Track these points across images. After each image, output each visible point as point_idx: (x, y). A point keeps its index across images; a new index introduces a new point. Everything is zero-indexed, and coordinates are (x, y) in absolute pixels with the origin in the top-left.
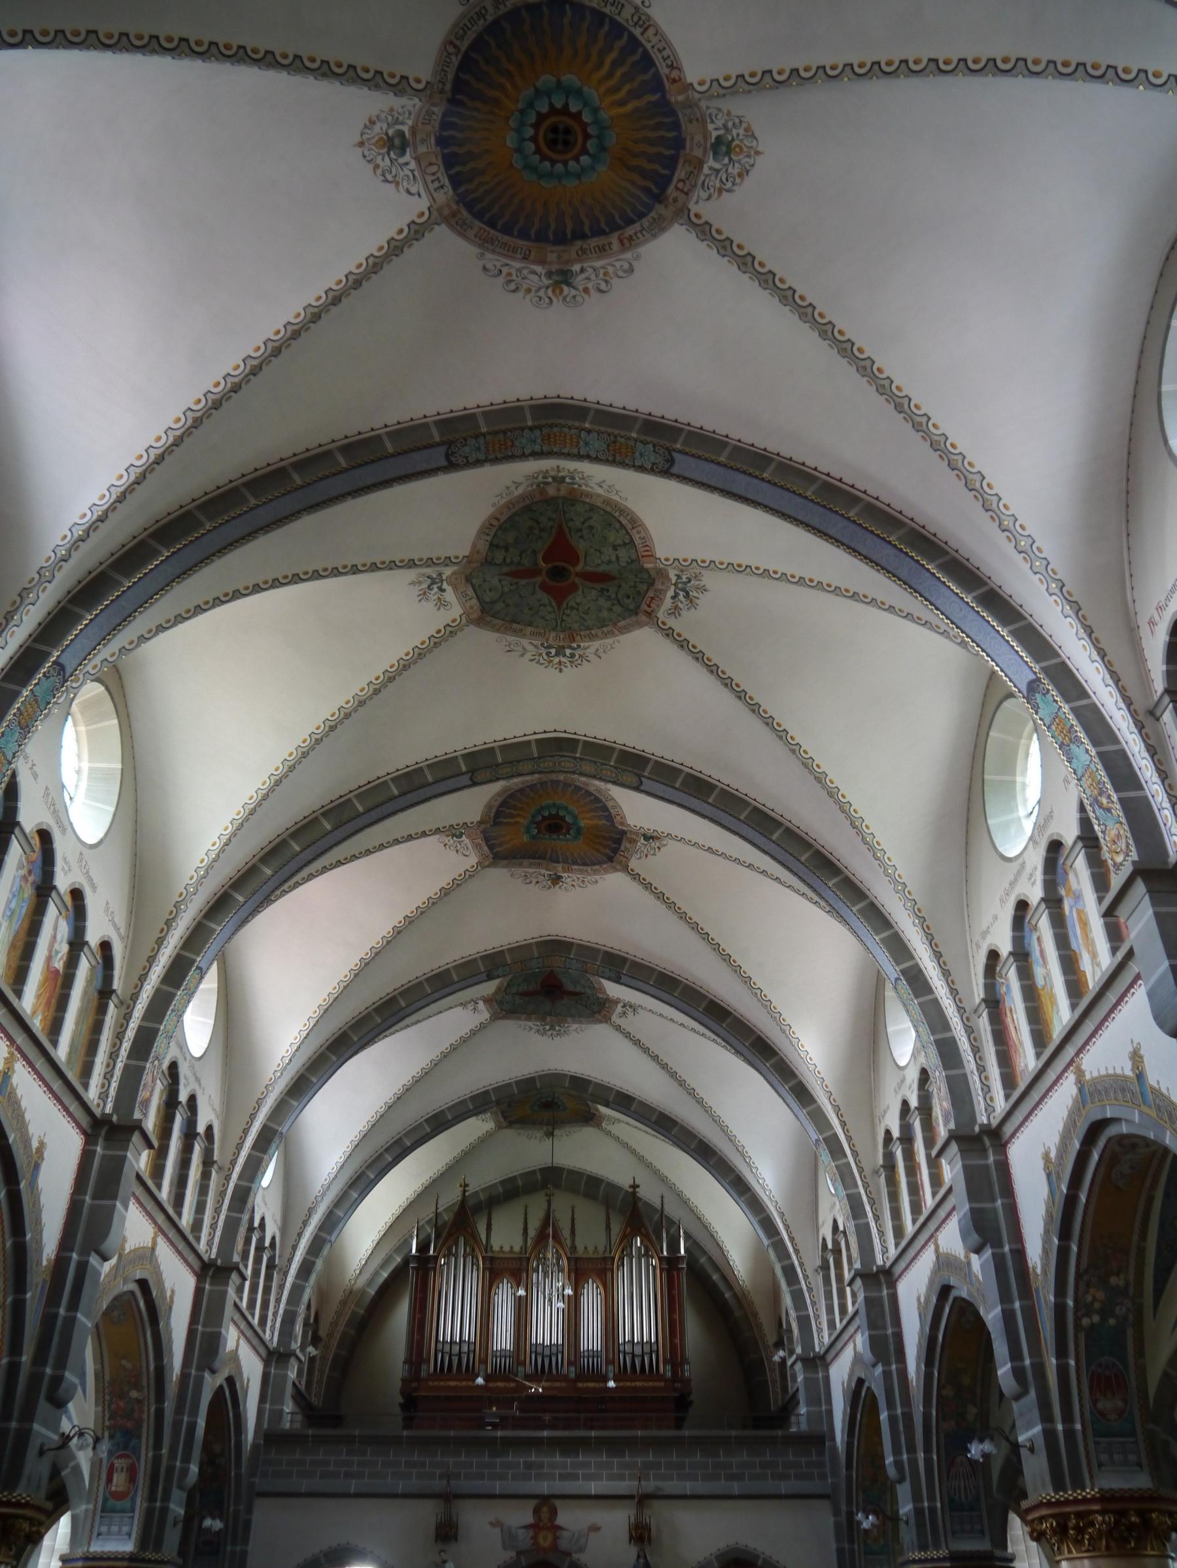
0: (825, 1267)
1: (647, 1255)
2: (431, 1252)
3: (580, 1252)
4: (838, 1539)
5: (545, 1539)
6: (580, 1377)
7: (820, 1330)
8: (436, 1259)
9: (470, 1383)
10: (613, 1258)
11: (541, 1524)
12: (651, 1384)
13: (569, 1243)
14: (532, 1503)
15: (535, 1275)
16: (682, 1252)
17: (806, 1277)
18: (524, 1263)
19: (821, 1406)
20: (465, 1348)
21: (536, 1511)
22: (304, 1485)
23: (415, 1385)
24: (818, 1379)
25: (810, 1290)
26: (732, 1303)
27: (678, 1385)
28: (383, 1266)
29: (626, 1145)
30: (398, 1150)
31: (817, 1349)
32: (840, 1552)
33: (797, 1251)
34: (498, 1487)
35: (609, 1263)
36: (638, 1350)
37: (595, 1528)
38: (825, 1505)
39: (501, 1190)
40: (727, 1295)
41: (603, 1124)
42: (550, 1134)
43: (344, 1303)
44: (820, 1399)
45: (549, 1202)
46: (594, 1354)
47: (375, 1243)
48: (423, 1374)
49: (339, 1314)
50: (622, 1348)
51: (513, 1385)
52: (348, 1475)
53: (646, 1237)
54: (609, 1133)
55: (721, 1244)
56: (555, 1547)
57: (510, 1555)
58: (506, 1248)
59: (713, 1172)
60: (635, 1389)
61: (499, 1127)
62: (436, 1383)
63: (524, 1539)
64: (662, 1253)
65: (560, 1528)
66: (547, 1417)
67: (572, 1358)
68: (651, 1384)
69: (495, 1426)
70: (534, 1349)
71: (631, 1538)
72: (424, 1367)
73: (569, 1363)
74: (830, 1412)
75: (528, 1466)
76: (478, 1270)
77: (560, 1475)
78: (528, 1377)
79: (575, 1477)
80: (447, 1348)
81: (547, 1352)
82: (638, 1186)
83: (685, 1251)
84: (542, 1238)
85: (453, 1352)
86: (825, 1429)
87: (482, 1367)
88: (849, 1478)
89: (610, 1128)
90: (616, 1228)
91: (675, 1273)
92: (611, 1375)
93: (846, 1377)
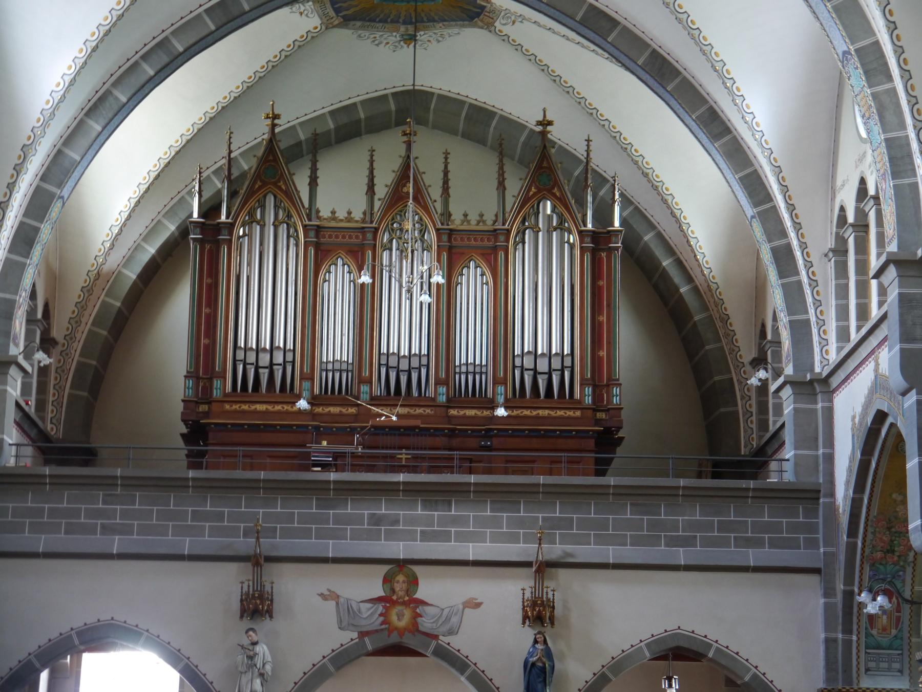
0: (840, 251)
1: (560, 227)
2: (223, 218)
3: (457, 221)
4: (828, 626)
5: (400, 616)
6: (452, 402)
7: (824, 343)
8: (231, 227)
9: (287, 407)
10: (509, 231)
11: (395, 598)
12: (560, 413)
13: (439, 206)
14: (385, 568)
15: (386, 254)
16: (617, 223)
17: (809, 265)
18: (369, 236)
19: (817, 449)
20: (279, 358)
21: (388, 580)
22: (42, 543)
23: (203, 408)
24: (816, 410)
25: (814, 283)
26: (691, 301)
27: (601, 415)
28: (147, 237)
29: (533, 58)
30: (165, 59)
31: (817, 370)
32: (830, 643)
33: (798, 226)
34: (331, 548)
35: (502, 238)
36: (543, 366)
37: (476, 605)
38: (814, 579)
39: (331, 125)
40: (683, 290)
41: (497, 24)
42: (411, 39)
43: (88, 290)
44: (817, 439)
45: (409, 145)
46: (476, 370)
47: (133, 202)
48: (216, 393)
49: (82, 306)
50: (518, 362)
51: (352, 410)
52: (106, 529)
53: (561, 201)
54: (506, 38)
55: (678, 213)
56: (414, 628)
57: (348, 637)
58: (341, 215)
59: (673, 103)
60: (537, 417)
61: (328, 26)
62: (236, 407)
63: (371, 617)
64: (585, 225)
65: (422, 603)
66: (404, 455)
67: (443, 375)
68: (560, 413)
69: (325, 466)
70: (383, 361)
71: (525, 618)
72: (217, 383)
73: (438, 383)
74: (830, 459)
75: (376, 520)
76: (297, 245)
77: (422, 532)
78: (374, 400)
79: (444, 537)
80: (251, 358)
81: (404, 365)
82: (550, 123)
83: (623, 222)
84: (397, 198)
86: (821, 481)
87: (306, 385)
88: (851, 548)
89: (507, 30)
90: (514, 187)
91: (604, 255)
92: (501, 399)
93: (859, 410)
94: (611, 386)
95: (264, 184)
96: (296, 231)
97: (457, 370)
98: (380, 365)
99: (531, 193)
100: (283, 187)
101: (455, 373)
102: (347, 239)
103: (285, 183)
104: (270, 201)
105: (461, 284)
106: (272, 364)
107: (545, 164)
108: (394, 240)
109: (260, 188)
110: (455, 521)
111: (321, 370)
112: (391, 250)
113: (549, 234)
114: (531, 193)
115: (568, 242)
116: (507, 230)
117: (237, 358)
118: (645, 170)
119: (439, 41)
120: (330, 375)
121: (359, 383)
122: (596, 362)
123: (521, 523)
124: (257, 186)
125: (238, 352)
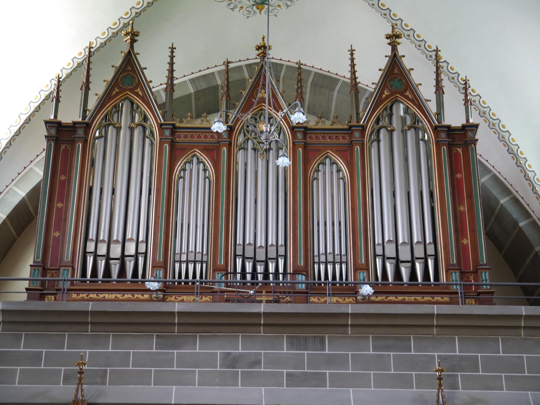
10: (363, 128)
15: (241, 154)
20: (131, 249)
35: (357, 135)
55: (515, 148)
70: (239, 252)
76: (152, 144)
85: (112, 255)
91: (460, 150)
94: (479, 271)
95: (122, 90)
96: (152, 133)
97: (316, 260)
98: (235, 256)
99: (384, 96)
100: (140, 93)
101: (314, 263)
102: (203, 139)
103: (142, 90)
104: (126, 108)
105: (317, 179)
106: (123, 257)
107: (396, 71)
108: (250, 142)
109: (117, 94)
110: (331, 361)
111: (175, 261)
112: (245, 149)
113: (404, 132)
114: (384, 96)
115: (423, 139)
116: (362, 126)
117: (88, 251)
118: (482, 109)
119: (288, 6)
120: (184, 266)
121: (214, 271)
122: (461, 250)
123: (413, 363)
124: (114, 93)
125: (88, 244)
